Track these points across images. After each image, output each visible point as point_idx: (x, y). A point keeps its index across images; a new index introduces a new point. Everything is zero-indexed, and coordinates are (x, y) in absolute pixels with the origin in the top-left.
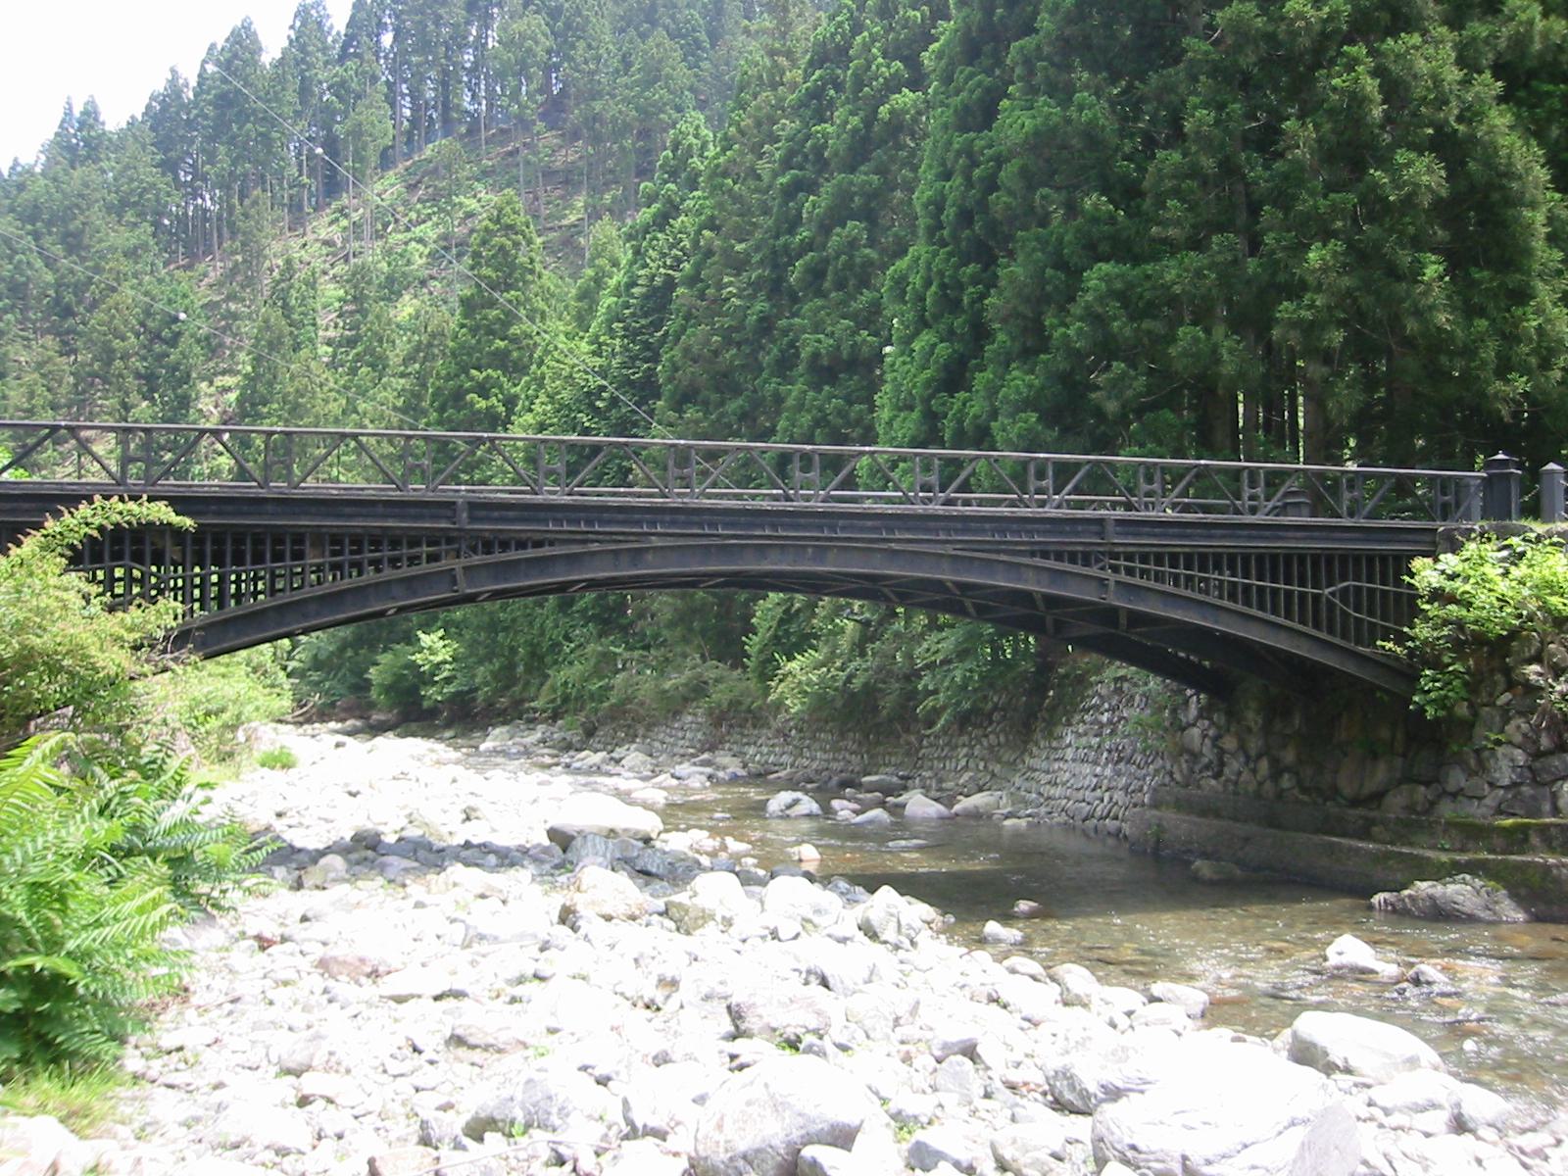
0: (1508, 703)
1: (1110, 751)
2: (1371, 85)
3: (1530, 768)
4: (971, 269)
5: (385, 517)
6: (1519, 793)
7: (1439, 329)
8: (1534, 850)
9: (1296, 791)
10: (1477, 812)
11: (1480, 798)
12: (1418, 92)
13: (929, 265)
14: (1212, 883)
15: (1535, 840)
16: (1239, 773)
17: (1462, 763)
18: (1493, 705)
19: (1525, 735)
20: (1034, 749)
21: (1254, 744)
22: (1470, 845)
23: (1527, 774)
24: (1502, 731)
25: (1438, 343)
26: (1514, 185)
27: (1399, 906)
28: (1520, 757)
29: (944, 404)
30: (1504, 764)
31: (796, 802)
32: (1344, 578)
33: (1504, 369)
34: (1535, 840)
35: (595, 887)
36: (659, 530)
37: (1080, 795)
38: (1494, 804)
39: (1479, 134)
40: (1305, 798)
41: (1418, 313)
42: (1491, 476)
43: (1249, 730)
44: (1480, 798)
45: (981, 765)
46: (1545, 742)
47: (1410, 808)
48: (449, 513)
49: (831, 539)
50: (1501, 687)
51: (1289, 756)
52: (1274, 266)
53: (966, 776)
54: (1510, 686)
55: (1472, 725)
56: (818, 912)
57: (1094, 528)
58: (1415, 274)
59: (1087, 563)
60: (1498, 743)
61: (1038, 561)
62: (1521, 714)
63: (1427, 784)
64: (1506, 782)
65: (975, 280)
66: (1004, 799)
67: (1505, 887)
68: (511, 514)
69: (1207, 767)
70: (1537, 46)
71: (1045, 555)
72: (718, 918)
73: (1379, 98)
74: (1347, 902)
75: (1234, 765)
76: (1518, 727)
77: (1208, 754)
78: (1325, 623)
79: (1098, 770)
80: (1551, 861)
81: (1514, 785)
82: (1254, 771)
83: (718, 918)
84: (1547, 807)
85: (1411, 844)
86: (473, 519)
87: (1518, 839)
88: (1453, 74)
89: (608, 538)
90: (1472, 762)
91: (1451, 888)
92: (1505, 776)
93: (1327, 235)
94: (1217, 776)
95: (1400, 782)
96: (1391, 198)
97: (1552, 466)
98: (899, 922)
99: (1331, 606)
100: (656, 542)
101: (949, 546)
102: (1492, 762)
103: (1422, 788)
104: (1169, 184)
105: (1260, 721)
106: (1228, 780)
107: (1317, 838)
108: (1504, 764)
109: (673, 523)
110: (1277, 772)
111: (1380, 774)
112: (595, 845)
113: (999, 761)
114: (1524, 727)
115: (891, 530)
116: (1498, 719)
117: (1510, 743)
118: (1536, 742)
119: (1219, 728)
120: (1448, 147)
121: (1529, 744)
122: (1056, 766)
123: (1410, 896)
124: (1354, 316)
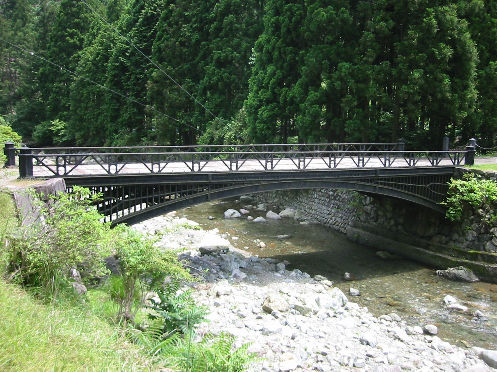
0: (473, 219)
1: (334, 204)
2: (434, 22)
3: (477, 237)
4: (290, 48)
5: (187, 180)
6: (474, 243)
7: (447, 97)
8: (479, 261)
9: (403, 231)
10: (462, 247)
11: (462, 243)
12: (448, 26)
13: (275, 44)
14: (385, 260)
15: (479, 257)
16: (384, 222)
17: (458, 233)
18: (468, 218)
19: (477, 228)
20: (301, 196)
21: (389, 215)
22: (460, 256)
23: (477, 238)
24: (470, 226)
25: (444, 100)
26: (469, 55)
27: (445, 275)
28: (475, 234)
29: (279, 91)
30: (470, 235)
31: (234, 213)
32: (431, 182)
33: (461, 108)
34: (479, 257)
35: (274, 301)
36: (264, 179)
37: (323, 215)
38: (466, 245)
39: (462, 39)
40: (406, 233)
41: (441, 92)
42: (469, 152)
43: (387, 211)
44: (462, 243)
45: (281, 197)
46: (482, 231)
47: (441, 242)
48: (206, 177)
49: (308, 179)
50: (471, 214)
51: (401, 220)
52: (400, 73)
53: (276, 200)
54: (474, 214)
55: (462, 223)
56: (334, 305)
57: (374, 172)
58: (441, 81)
59: (371, 182)
60: (469, 229)
61: (359, 183)
62: (476, 222)
63: (446, 237)
64: (470, 240)
65: (291, 53)
66: (296, 213)
67: (472, 271)
68: (223, 177)
69: (372, 218)
70: (477, 10)
71: (361, 180)
72: (313, 311)
73: (436, 26)
74: (426, 270)
75: (381, 220)
76: (475, 225)
77: (373, 214)
78: (426, 195)
79: (329, 209)
80: (486, 265)
81: (472, 241)
82: (389, 223)
83: (313, 311)
84: (482, 248)
85: (442, 253)
86: (213, 179)
87: (474, 257)
88: (456, 20)
89: (249, 182)
90: (461, 233)
91: (460, 271)
92: (470, 238)
93: (418, 67)
94: (375, 221)
95: (436, 235)
96: (438, 58)
97: (473, 139)
98: (342, 299)
99: (428, 189)
100: (263, 183)
101: (338, 180)
102: (467, 234)
103: (444, 237)
104: (369, 44)
105: (391, 209)
106: (379, 223)
107: (412, 247)
108: (470, 235)
109: (267, 177)
110: (397, 224)
111: (432, 231)
112: (234, 265)
113: (287, 196)
114: (477, 226)
115: (324, 176)
116: (469, 223)
117: (472, 229)
118: (480, 230)
119: (377, 208)
120: (453, 43)
121: (478, 230)
122: (311, 203)
123: (448, 272)
124: (423, 92)
